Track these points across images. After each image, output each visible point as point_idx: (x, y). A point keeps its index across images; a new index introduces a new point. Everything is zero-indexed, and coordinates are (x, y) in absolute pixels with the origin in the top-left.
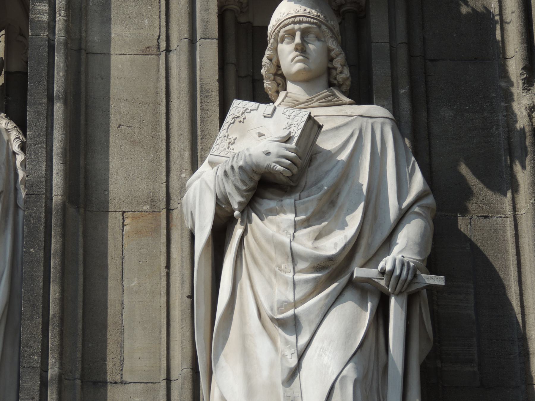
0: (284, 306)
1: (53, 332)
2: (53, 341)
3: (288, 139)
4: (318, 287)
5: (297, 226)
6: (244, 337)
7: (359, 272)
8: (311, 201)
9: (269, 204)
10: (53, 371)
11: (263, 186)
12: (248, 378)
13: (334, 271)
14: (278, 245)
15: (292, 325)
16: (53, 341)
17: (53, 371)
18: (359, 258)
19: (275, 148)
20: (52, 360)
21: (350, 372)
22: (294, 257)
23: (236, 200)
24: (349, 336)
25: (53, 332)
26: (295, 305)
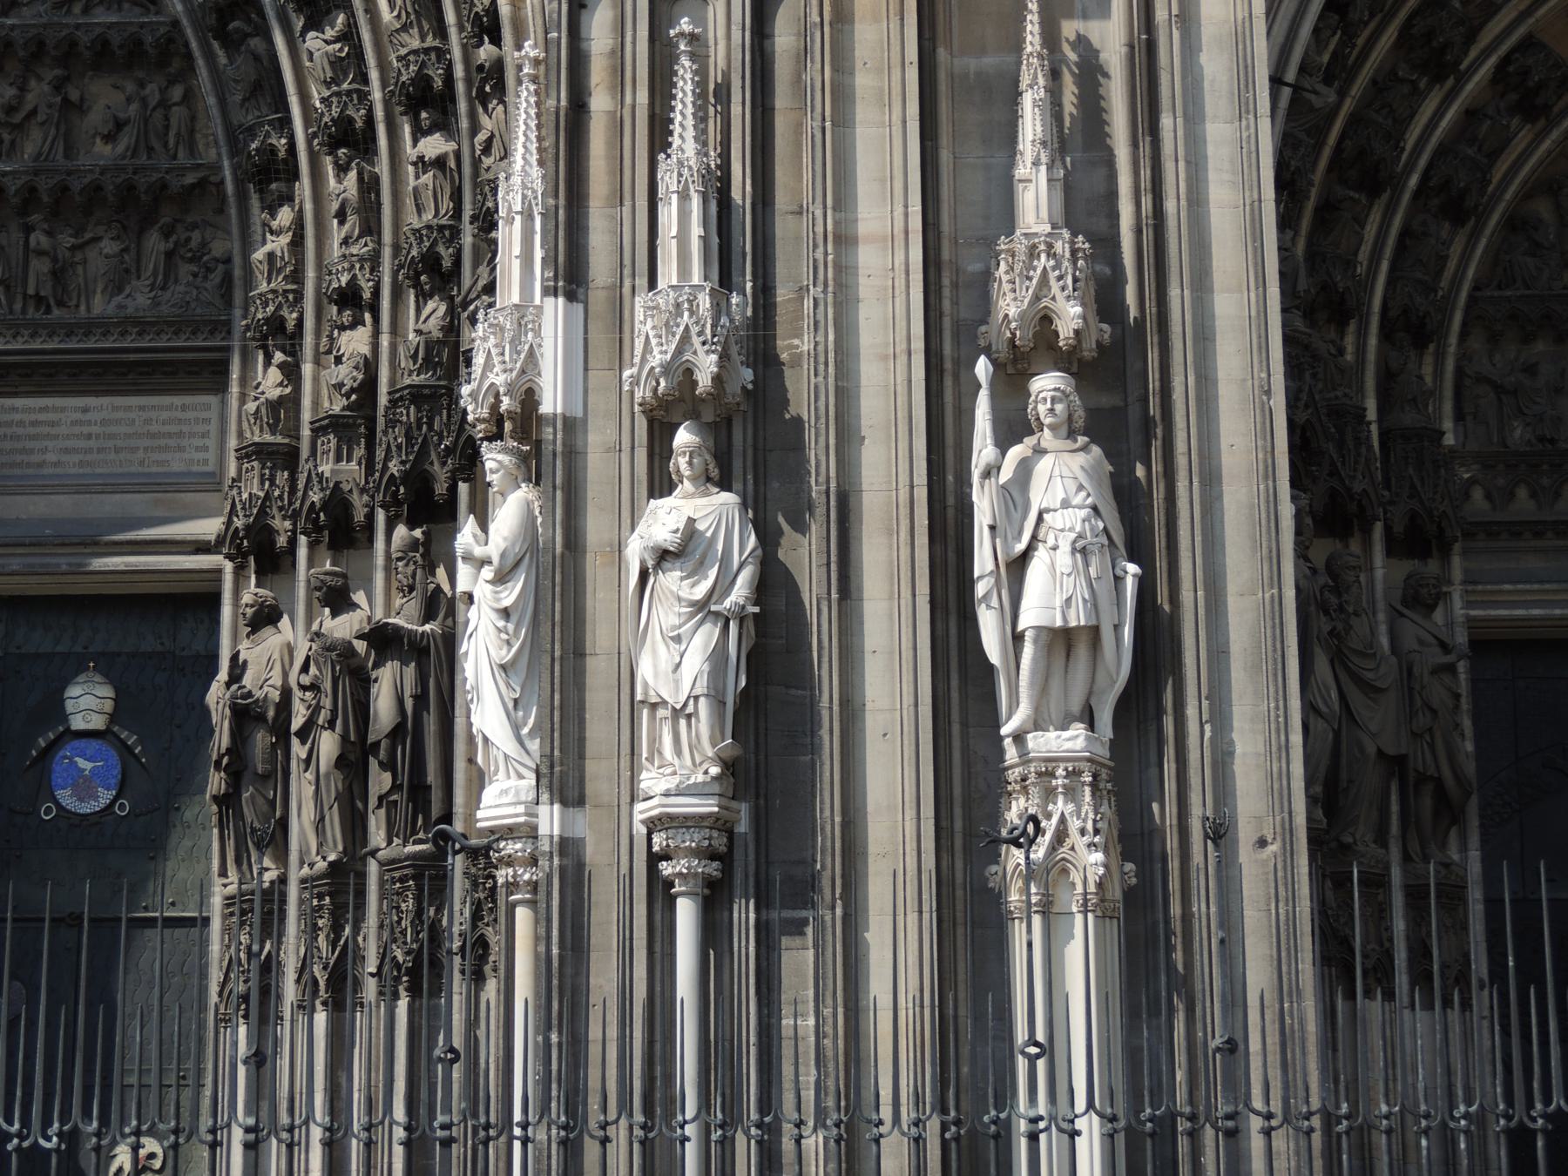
0: (674, 628)
1: (557, 630)
2: (558, 636)
3: (676, 531)
4: (692, 615)
5: (682, 579)
6: (654, 643)
7: (713, 608)
8: (690, 565)
9: (666, 565)
10: (557, 654)
11: (664, 556)
12: (655, 666)
13: (701, 607)
14: (672, 592)
15: (677, 639)
16: (558, 636)
17: (557, 654)
18: (714, 599)
19: (669, 537)
20: (557, 646)
21: (706, 667)
22: (679, 599)
23: (650, 563)
24: (706, 646)
25: (557, 630)
26: (680, 627)
